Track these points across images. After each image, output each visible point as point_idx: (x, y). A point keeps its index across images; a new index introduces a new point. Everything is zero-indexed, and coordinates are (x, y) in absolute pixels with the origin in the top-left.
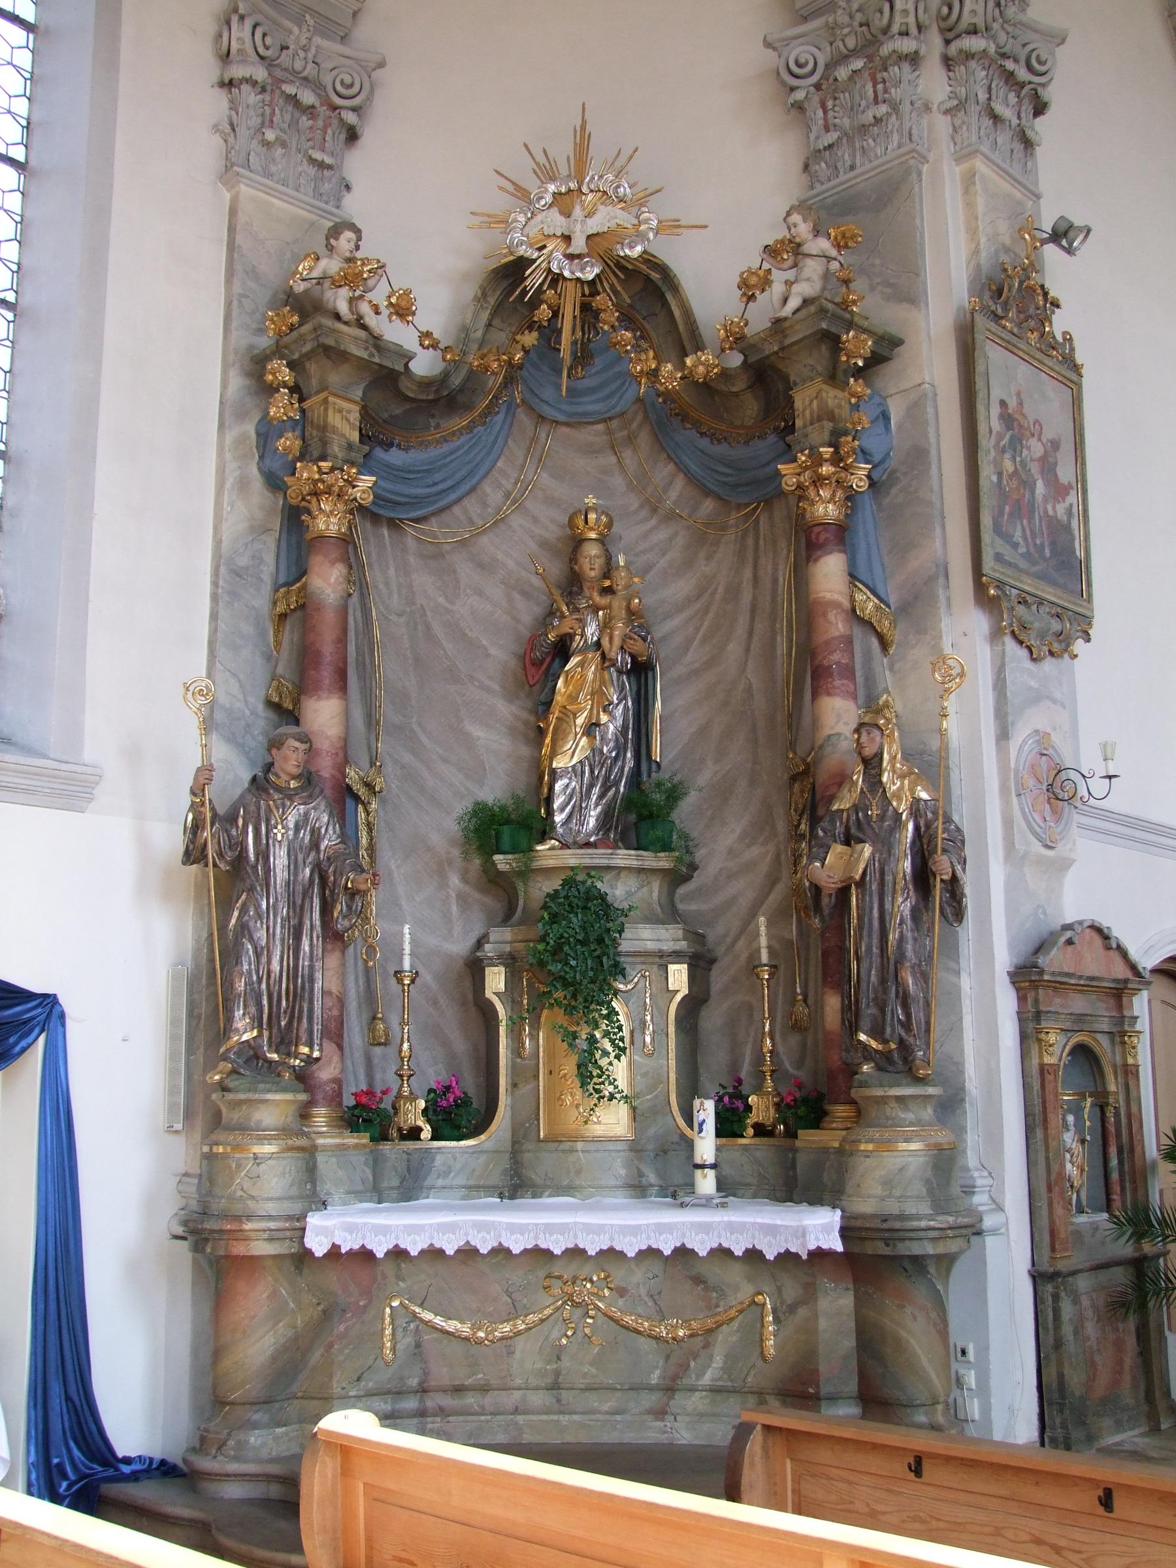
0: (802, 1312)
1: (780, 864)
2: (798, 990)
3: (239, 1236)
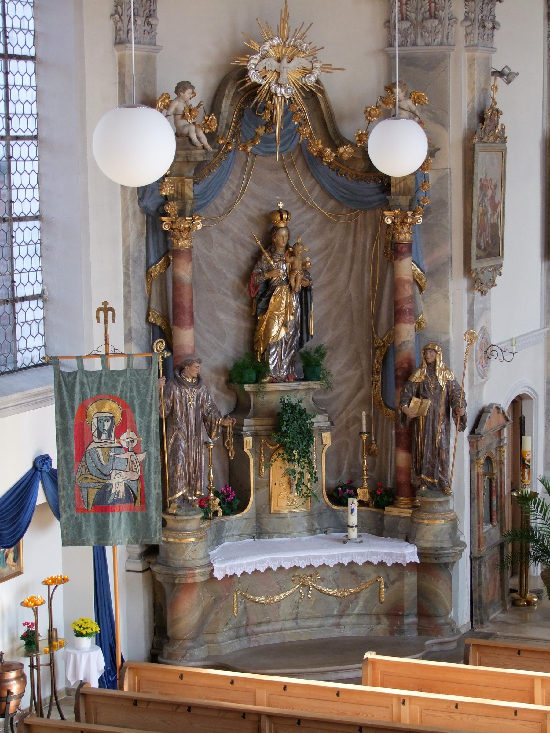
0: (397, 584)
1: (363, 380)
2: (373, 439)
3: (193, 576)
